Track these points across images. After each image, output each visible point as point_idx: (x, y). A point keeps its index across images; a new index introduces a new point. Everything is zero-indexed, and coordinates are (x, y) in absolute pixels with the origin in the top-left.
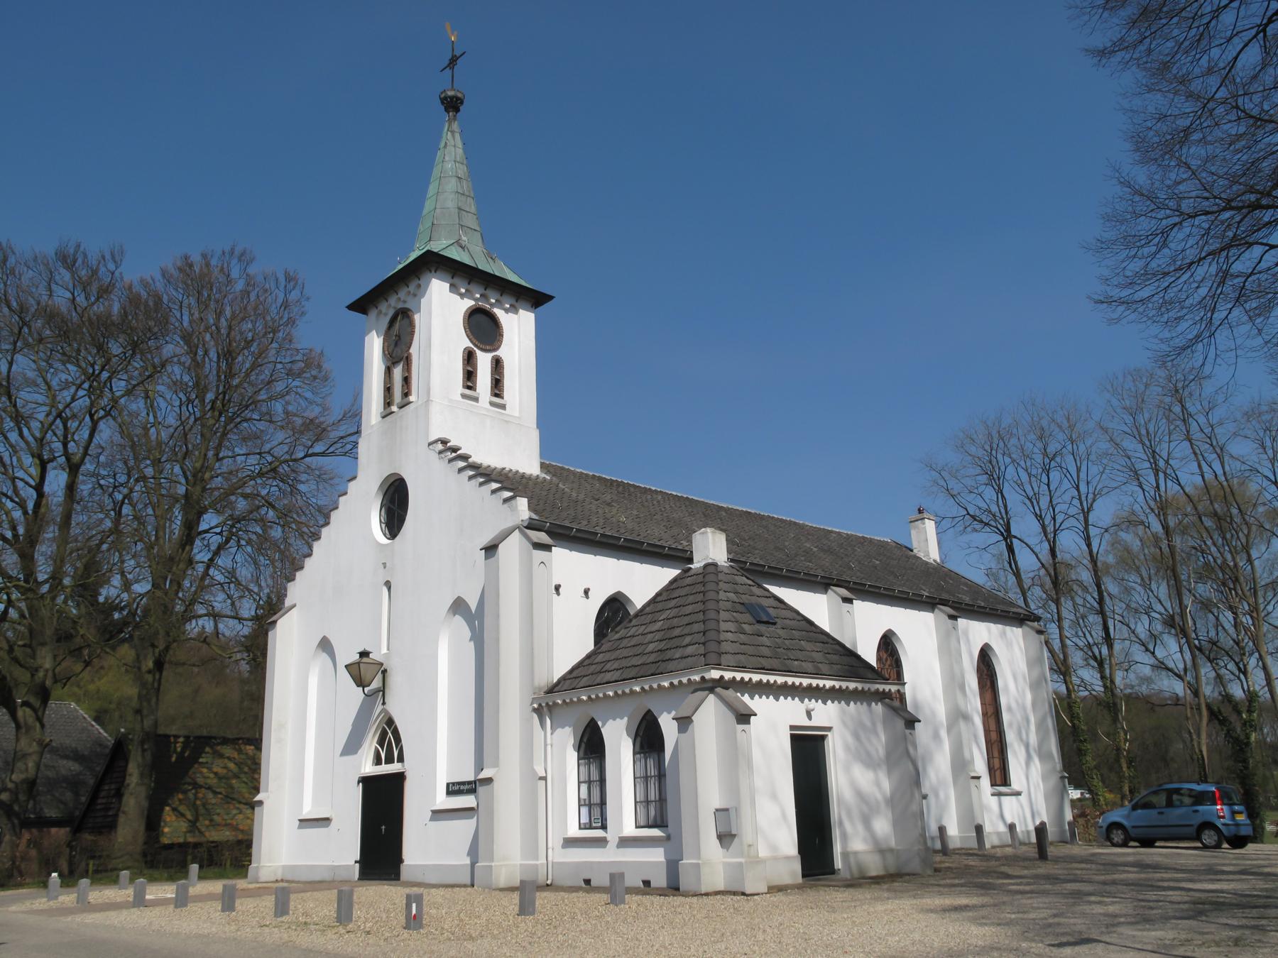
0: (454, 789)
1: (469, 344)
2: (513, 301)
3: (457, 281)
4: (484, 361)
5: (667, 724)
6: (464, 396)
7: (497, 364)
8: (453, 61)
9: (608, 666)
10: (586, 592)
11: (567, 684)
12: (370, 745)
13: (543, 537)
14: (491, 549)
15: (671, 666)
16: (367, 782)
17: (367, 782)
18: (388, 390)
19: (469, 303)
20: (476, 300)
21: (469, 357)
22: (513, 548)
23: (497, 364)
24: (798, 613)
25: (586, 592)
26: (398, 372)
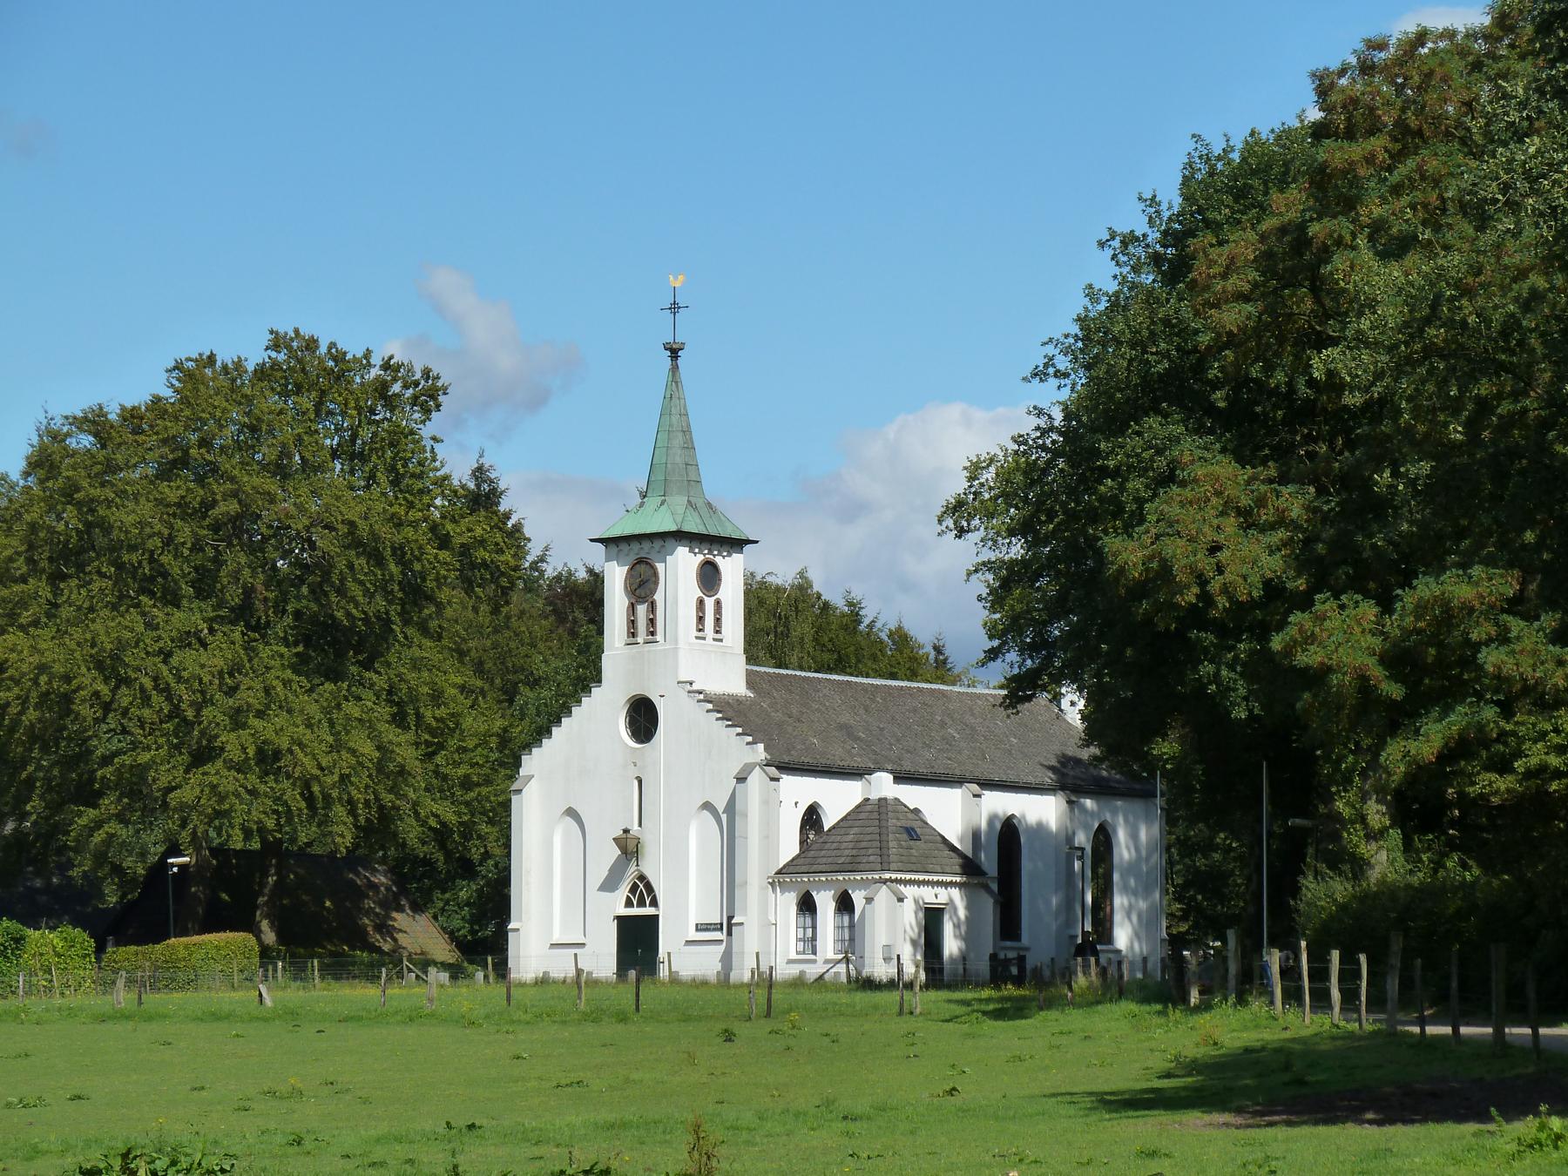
0: (700, 928)
1: (702, 595)
2: (728, 548)
3: (693, 544)
4: (709, 603)
5: (858, 897)
6: (697, 638)
7: (718, 603)
8: (675, 308)
9: (819, 860)
10: (796, 803)
11: (791, 869)
12: (623, 891)
13: (773, 771)
14: (741, 779)
15: (861, 867)
16: (622, 921)
17: (622, 921)
18: (632, 623)
19: (700, 558)
20: (704, 555)
21: (701, 603)
22: (756, 777)
23: (718, 603)
24: (934, 829)
25: (796, 803)
26: (642, 609)
